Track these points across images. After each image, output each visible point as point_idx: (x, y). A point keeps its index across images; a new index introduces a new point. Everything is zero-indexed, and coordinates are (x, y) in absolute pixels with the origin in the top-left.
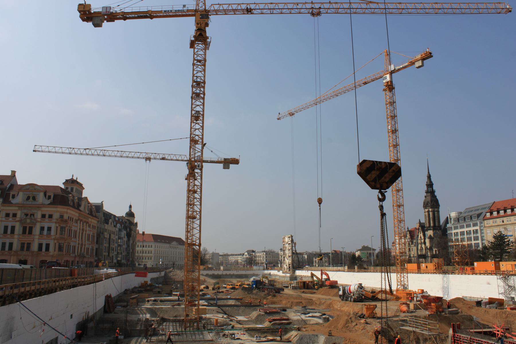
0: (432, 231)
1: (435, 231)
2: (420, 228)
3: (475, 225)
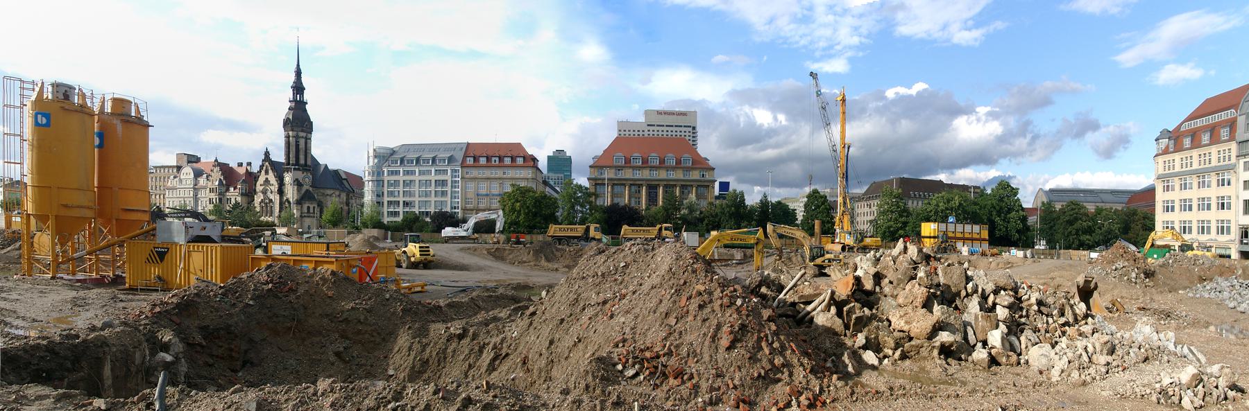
0: (301, 172)
1: (305, 174)
2: (267, 163)
3: (407, 173)
